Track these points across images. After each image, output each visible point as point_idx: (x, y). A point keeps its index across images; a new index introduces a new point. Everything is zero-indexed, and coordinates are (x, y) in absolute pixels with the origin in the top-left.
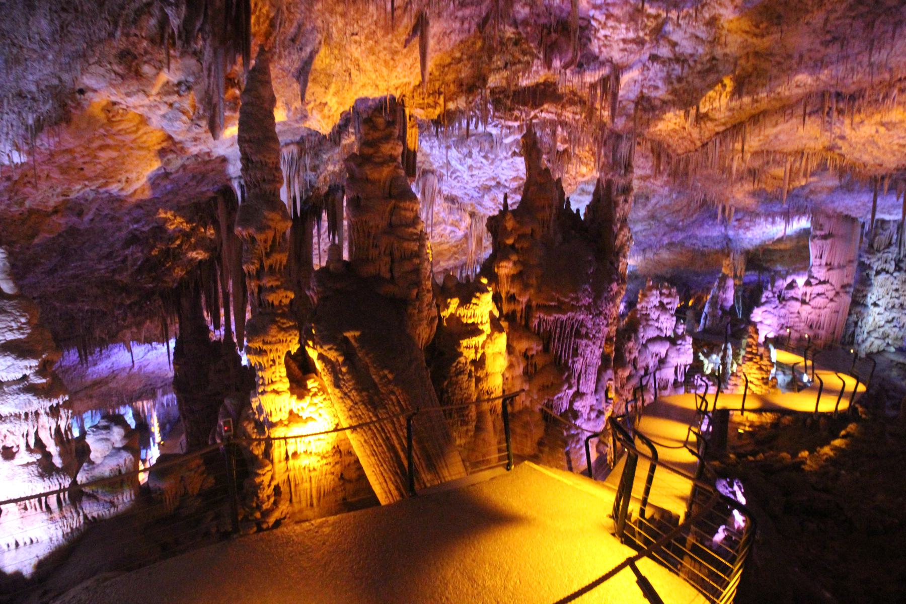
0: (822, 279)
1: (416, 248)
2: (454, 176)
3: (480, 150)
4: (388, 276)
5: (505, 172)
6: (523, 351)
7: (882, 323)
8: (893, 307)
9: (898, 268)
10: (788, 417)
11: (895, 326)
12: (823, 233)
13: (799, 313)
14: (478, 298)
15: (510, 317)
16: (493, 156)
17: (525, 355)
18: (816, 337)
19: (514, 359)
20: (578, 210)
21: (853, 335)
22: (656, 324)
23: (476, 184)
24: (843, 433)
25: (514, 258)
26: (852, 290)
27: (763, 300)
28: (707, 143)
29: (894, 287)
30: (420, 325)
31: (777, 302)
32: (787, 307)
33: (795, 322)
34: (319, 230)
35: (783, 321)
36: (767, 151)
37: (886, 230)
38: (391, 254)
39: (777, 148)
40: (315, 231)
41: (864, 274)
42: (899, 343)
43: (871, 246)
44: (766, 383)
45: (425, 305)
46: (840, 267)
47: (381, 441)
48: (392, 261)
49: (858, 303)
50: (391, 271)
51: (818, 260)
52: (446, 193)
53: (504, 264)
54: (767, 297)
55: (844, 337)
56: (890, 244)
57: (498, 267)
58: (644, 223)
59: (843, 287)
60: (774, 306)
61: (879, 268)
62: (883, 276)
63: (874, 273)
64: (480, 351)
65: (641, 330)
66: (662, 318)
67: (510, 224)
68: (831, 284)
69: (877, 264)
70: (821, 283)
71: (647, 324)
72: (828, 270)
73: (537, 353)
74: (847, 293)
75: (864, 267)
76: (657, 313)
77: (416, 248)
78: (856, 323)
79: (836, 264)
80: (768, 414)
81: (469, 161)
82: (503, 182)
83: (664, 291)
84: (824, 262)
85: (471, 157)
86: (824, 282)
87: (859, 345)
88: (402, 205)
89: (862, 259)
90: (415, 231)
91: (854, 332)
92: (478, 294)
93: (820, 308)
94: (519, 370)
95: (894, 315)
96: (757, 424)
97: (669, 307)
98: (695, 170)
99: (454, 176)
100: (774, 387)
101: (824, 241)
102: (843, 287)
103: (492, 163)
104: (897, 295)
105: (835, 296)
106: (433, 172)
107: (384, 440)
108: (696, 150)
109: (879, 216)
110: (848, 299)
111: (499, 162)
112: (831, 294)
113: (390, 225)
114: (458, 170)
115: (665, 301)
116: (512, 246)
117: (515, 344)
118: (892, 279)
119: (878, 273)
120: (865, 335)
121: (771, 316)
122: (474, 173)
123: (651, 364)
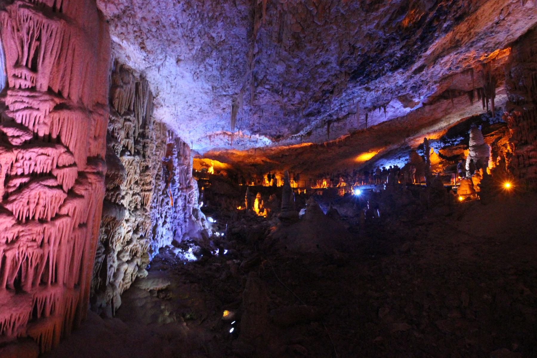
0: (42, 132)
8: (136, 208)
11: (142, 237)
18: (36, 317)
29: (137, 177)
37: (125, 84)
46: (82, 108)
49: (111, 204)
56: (129, 112)
59: (92, 161)
68: (68, 151)
70: (37, 141)
72: (58, 108)
84: (43, 83)
86: (49, 141)
87: (112, 285)
93: (42, 221)
95: (140, 220)
102: (92, 161)
104: (137, 189)
105: (77, 182)
112: (68, 177)
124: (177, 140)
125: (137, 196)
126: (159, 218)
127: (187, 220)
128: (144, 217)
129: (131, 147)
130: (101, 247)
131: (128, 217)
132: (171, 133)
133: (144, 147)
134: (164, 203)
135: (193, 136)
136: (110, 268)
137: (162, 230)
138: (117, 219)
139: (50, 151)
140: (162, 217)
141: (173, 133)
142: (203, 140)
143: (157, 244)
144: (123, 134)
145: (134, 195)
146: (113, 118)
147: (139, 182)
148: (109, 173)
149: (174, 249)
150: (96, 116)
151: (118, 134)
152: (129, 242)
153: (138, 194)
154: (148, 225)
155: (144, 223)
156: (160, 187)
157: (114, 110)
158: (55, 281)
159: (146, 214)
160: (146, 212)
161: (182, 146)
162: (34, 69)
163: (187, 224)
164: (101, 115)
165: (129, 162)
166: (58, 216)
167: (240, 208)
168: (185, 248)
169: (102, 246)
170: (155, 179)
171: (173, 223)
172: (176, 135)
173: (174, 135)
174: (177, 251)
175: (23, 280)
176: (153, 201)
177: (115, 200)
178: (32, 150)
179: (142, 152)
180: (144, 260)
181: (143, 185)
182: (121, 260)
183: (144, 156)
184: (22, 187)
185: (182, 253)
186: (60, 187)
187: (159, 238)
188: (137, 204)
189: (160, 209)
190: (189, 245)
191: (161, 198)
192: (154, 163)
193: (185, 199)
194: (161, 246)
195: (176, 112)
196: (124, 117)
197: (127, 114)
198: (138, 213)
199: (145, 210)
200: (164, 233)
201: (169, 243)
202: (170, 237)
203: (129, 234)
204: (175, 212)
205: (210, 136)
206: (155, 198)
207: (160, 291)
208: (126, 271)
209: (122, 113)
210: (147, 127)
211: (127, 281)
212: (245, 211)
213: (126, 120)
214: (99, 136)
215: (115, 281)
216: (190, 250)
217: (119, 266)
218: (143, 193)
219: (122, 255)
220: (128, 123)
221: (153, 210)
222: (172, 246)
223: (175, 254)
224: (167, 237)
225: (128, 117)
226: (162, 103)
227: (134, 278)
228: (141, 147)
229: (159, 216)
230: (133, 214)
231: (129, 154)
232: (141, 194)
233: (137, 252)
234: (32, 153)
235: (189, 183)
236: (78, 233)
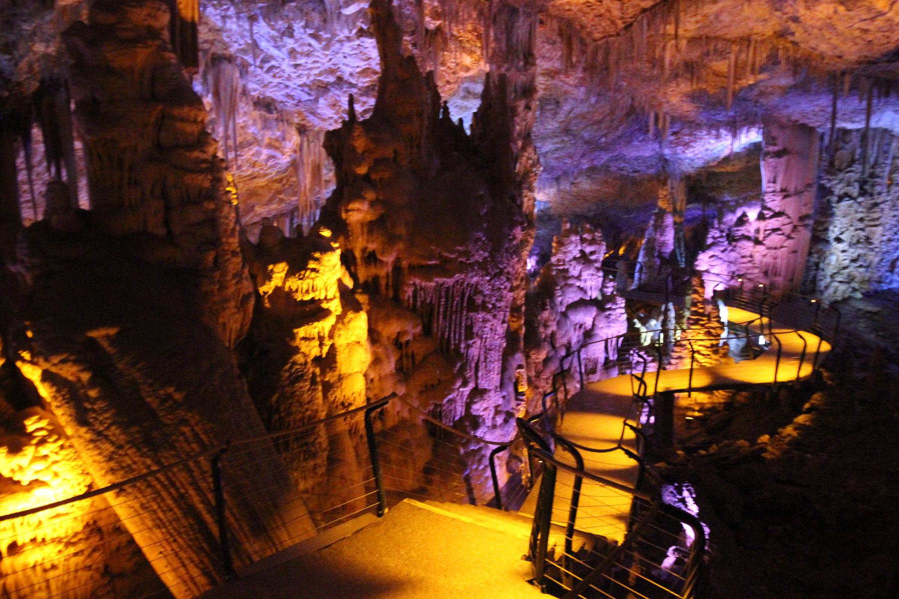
0: (777, 210)
1: (207, 184)
2: (267, 66)
3: (306, 26)
4: (161, 231)
5: (349, 61)
6: (394, 337)
7: (847, 262)
8: (858, 242)
9: (863, 193)
10: (744, 393)
11: (861, 266)
12: (776, 148)
13: (751, 256)
14: (317, 260)
15: (370, 287)
16: (328, 36)
17: (398, 343)
18: (772, 286)
19: (380, 350)
20: (461, 120)
21: (814, 281)
22: (578, 284)
23: (304, 80)
24: (807, 406)
25: (370, 195)
26: (810, 222)
27: (710, 241)
28: (631, 25)
29: (859, 216)
30: (224, 309)
31: (726, 243)
32: (738, 249)
33: (748, 269)
34: (28, 158)
35: (733, 268)
36: (707, 37)
38: (164, 195)
39: (719, 33)
40: (20, 161)
41: (825, 200)
42: (866, 287)
43: (832, 164)
44: (716, 352)
45: (229, 277)
46: (798, 193)
47: (170, 502)
48: (167, 208)
49: (819, 240)
50: (166, 223)
51: (771, 185)
52: (255, 94)
53: (355, 205)
54: (713, 237)
55: (804, 284)
56: (853, 162)
57: (347, 211)
58: (555, 140)
60: (722, 249)
61: (842, 192)
62: (844, 204)
63: (835, 199)
64: (328, 343)
65: (559, 293)
66: (585, 275)
67: (360, 144)
69: (839, 186)
71: (566, 285)
72: (785, 197)
73: (414, 338)
74: (806, 226)
75: (824, 192)
76: (579, 268)
77: (207, 184)
78: (817, 264)
79: (792, 190)
80: (721, 392)
81: (290, 43)
82: (346, 77)
83: (585, 236)
84: (778, 187)
85: (291, 36)
87: (822, 292)
88: (176, 112)
89: (822, 182)
90: (203, 156)
91: (815, 277)
92: (317, 255)
93: (775, 248)
94: (389, 366)
95: (860, 251)
96: (708, 406)
97: (593, 257)
98: (617, 63)
99: (267, 66)
100: (725, 355)
101: (777, 160)
102: (802, 219)
103: (326, 48)
104: (861, 225)
105: (793, 231)
106: (230, 59)
107: (175, 500)
108: (618, 35)
109: (840, 124)
110: (805, 235)
111: (338, 45)
112: (787, 229)
113: (159, 146)
114: (272, 58)
115: (588, 250)
116: (366, 178)
117: (380, 328)
118: (856, 205)
119: (841, 199)
120: (828, 280)
121: (719, 262)
122: (298, 62)
123: (574, 340)
139: (779, 219)
150: (806, 193)
152: (845, 268)
162: (774, 182)
166: (782, 247)
184: (769, 234)
186: (783, 234)
198: (860, 245)
207: (868, 312)
233: (855, 278)
234: (773, 220)
236: (791, 255)
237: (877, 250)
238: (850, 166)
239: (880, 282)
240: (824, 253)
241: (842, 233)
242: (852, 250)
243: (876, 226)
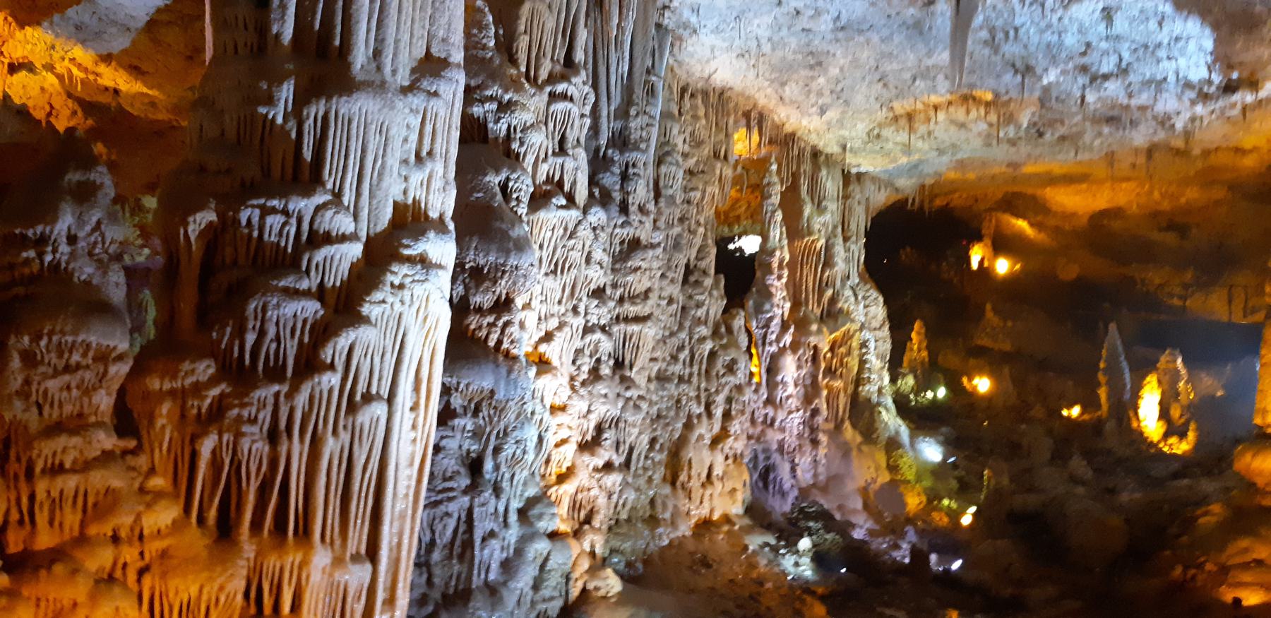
9: (599, 197)
29: (597, 276)
41: (494, 179)
62: (553, 217)
78: (474, 466)
89: (477, 110)
95: (603, 410)
119: (539, 199)
124: (785, 141)
125: (598, 335)
126: (699, 416)
127: (823, 438)
128: (620, 405)
129: (574, 183)
130: (459, 472)
131: (564, 398)
132: (755, 118)
133: (625, 177)
134: (719, 366)
135: (841, 123)
136: (484, 540)
137: (700, 457)
138: (500, 395)
140: (710, 415)
141: (761, 119)
142: (887, 132)
143: (684, 504)
144: (538, 139)
145: (587, 330)
146: (507, 97)
147: (608, 291)
148: (482, 262)
149: (747, 530)
150: (417, 101)
151: (522, 144)
153: (603, 329)
154: (635, 431)
155: (621, 425)
156: (701, 313)
157: (513, 71)
158: (304, 532)
159: (628, 394)
160: (628, 388)
161: (807, 167)
163: (822, 451)
164: (436, 94)
165: (566, 229)
167: (1075, 411)
168: (788, 533)
169: (462, 470)
170: (685, 281)
171: (758, 440)
172: (779, 127)
173: (767, 126)
174: (755, 541)
175: (233, 514)
176: (674, 358)
177: (500, 342)
178: (255, 202)
179: (617, 196)
180: (616, 543)
181: (621, 300)
182: (531, 524)
183: (624, 209)
185: (775, 549)
187: (695, 484)
188: (598, 360)
189: (703, 385)
190: (802, 524)
191: (709, 345)
192: (677, 230)
193: (815, 358)
194: (704, 512)
195: (754, 44)
196: (548, 89)
197: (552, 79)
198: (601, 388)
199: (627, 382)
200: (718, 471)
201: (737, 509)
202: (739, 486)
203: (562, 449)
204: (769, 401)
205: (910, 117)
206: (681, 348)
208: (546, 559)
209: (543, 75)
210: (633, 112)
211: (546, 592)
212: (1096, 428)
213: (553, 97)
214: (430, 153)
215: (505, 583)
216: (805, 543)
217: (524, 540)
218: (622, 326)
219: (535, 511)
220: (560, 106)
221: (672, 389)
222: (747, 521)
223: (746, 548)
224: (729, 485)
225: (560, 88)
226: (694, 19)
227: (575, 592)
228: (617, 179)
229: (702, 409)
230: (582, 391)
231: (563, 202)
232: (615, 329)
235: (833, 300)
237: (644, 405)
238: (564, 78)
239: (653, 521)
240: (500, 410)
241: (548, 337)
242: (579, 405)
243: (638, 319)
